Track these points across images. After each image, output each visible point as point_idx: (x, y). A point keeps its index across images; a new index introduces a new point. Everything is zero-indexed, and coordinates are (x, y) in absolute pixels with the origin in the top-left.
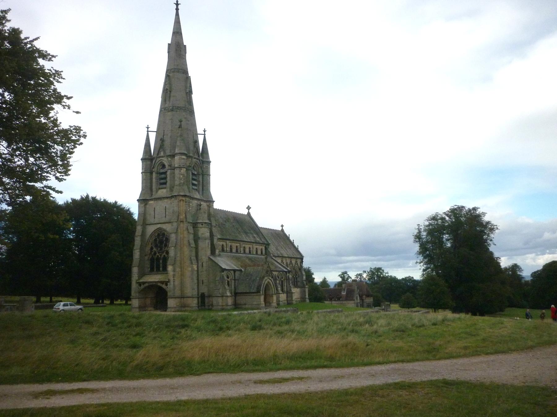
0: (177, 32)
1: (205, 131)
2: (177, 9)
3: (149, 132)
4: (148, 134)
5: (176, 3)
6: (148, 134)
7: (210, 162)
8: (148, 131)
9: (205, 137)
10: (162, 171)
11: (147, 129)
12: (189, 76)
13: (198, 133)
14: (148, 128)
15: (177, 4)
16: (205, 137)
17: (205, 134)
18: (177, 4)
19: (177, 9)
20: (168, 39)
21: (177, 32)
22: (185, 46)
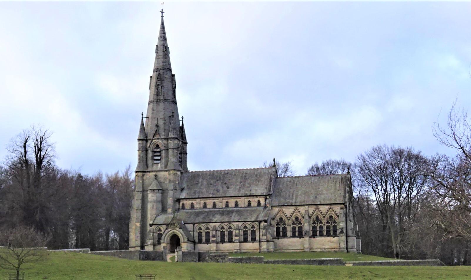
0: (163, 37)
1: (183, 118)
2: (162, 17)
3: (143, 118)
4: (142, 119)
5: (161, 11)
6: (142, 119)
7: (187, 143)
8: (142, 117)
9: (183, 123)
10: (156, 150)
11: (141, 115)
12: (173, 74)
13: (180, 120)
14: (142, 114)
15: (162, 12)
16: (183, 123)
17: (183, 121)
18: (162, 12)
19: (162, 17)
20: (155, 41)
21: (163, 37)
22: (169, 47)
